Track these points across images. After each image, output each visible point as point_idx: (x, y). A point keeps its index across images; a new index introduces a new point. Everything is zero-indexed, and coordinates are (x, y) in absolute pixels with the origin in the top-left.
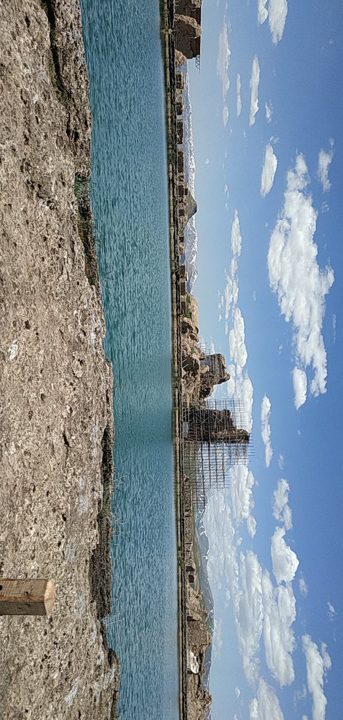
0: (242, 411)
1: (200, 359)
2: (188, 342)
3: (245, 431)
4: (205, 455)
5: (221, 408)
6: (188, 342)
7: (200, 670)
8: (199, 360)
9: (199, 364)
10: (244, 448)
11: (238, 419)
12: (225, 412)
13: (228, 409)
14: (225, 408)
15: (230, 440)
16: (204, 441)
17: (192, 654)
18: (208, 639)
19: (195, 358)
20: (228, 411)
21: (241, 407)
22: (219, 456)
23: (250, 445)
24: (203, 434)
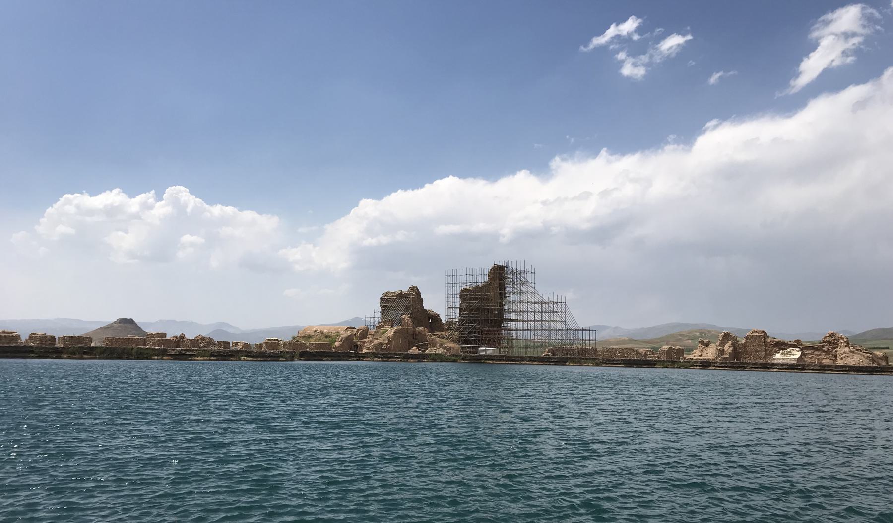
0: (464, 274)
1: (392, 326)
2: (371, 342)
3: (491, 270)
4: (519, 325)
5: (458, 301)
6: (371, 342)
7: (795, 346)
8: (395, 328)
9: (400, 327)
11: (473, 279)
12: (464, 295)
13: (459, 292)
14: (458, 296)
15: (502, 294)
16: (500, 326)
17: (778, 356)
18: (757, 334)
19: (392, 333)
20: (462, 291)
21: (458, 274)
22: (523, 307)
23: (523, 269)
24: (493, 327)
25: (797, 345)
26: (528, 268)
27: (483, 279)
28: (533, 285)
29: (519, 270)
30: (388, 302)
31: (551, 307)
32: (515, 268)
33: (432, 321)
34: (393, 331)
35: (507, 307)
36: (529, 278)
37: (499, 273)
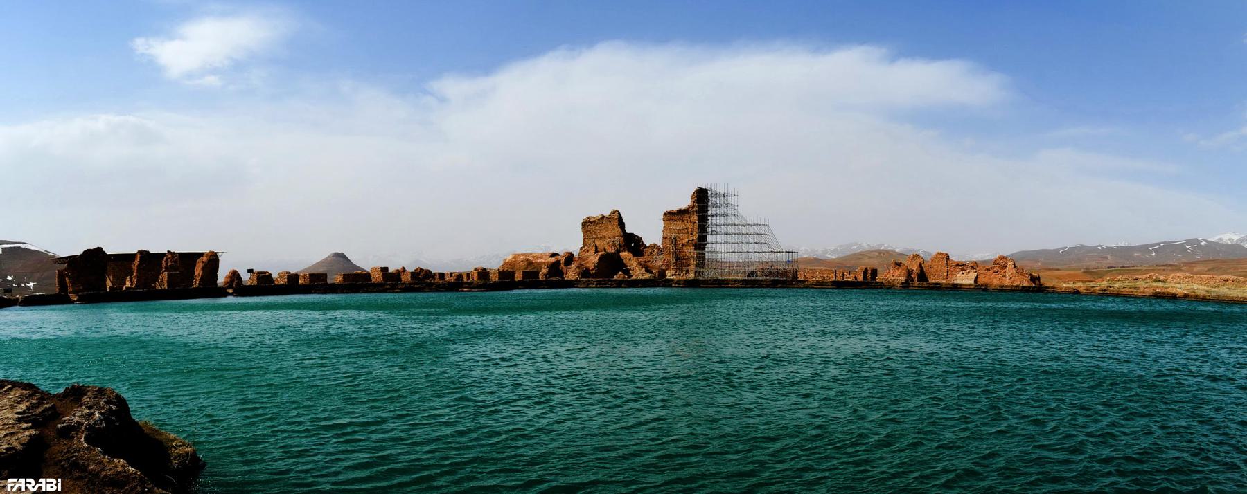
4: (717, 248)
10: (718, 195)
16: (704, 249)
19: (597, 259)
25: (974, 266)
26: (731, 191)
27: (685, 202)
28: (736, 208)
29: (722, 193)
30: (588, 225)
31: (755, 230)
32: (718, 190)
33: (633, 243)
34: (599, 256)
35: (709, 230)
36: (732, 200)
37: (702, 196)
